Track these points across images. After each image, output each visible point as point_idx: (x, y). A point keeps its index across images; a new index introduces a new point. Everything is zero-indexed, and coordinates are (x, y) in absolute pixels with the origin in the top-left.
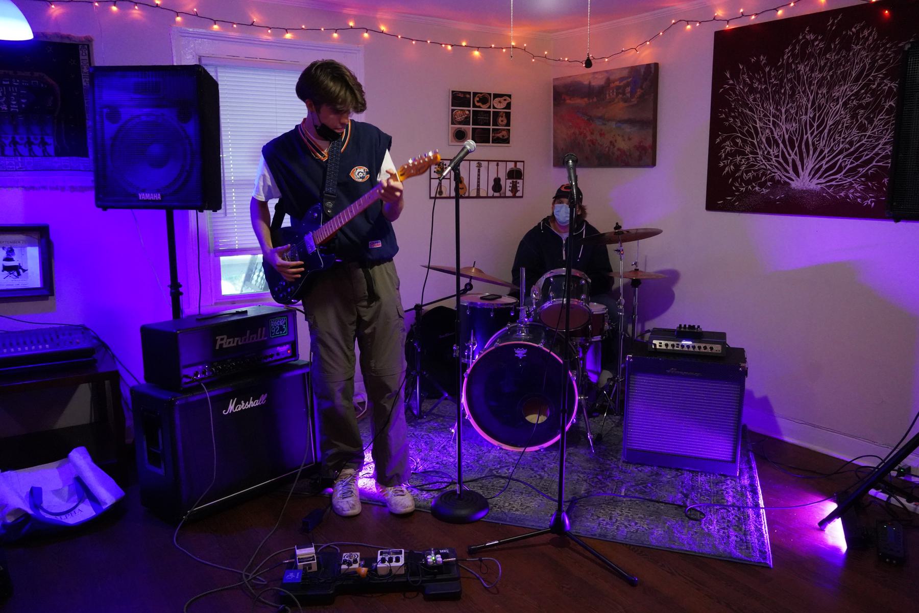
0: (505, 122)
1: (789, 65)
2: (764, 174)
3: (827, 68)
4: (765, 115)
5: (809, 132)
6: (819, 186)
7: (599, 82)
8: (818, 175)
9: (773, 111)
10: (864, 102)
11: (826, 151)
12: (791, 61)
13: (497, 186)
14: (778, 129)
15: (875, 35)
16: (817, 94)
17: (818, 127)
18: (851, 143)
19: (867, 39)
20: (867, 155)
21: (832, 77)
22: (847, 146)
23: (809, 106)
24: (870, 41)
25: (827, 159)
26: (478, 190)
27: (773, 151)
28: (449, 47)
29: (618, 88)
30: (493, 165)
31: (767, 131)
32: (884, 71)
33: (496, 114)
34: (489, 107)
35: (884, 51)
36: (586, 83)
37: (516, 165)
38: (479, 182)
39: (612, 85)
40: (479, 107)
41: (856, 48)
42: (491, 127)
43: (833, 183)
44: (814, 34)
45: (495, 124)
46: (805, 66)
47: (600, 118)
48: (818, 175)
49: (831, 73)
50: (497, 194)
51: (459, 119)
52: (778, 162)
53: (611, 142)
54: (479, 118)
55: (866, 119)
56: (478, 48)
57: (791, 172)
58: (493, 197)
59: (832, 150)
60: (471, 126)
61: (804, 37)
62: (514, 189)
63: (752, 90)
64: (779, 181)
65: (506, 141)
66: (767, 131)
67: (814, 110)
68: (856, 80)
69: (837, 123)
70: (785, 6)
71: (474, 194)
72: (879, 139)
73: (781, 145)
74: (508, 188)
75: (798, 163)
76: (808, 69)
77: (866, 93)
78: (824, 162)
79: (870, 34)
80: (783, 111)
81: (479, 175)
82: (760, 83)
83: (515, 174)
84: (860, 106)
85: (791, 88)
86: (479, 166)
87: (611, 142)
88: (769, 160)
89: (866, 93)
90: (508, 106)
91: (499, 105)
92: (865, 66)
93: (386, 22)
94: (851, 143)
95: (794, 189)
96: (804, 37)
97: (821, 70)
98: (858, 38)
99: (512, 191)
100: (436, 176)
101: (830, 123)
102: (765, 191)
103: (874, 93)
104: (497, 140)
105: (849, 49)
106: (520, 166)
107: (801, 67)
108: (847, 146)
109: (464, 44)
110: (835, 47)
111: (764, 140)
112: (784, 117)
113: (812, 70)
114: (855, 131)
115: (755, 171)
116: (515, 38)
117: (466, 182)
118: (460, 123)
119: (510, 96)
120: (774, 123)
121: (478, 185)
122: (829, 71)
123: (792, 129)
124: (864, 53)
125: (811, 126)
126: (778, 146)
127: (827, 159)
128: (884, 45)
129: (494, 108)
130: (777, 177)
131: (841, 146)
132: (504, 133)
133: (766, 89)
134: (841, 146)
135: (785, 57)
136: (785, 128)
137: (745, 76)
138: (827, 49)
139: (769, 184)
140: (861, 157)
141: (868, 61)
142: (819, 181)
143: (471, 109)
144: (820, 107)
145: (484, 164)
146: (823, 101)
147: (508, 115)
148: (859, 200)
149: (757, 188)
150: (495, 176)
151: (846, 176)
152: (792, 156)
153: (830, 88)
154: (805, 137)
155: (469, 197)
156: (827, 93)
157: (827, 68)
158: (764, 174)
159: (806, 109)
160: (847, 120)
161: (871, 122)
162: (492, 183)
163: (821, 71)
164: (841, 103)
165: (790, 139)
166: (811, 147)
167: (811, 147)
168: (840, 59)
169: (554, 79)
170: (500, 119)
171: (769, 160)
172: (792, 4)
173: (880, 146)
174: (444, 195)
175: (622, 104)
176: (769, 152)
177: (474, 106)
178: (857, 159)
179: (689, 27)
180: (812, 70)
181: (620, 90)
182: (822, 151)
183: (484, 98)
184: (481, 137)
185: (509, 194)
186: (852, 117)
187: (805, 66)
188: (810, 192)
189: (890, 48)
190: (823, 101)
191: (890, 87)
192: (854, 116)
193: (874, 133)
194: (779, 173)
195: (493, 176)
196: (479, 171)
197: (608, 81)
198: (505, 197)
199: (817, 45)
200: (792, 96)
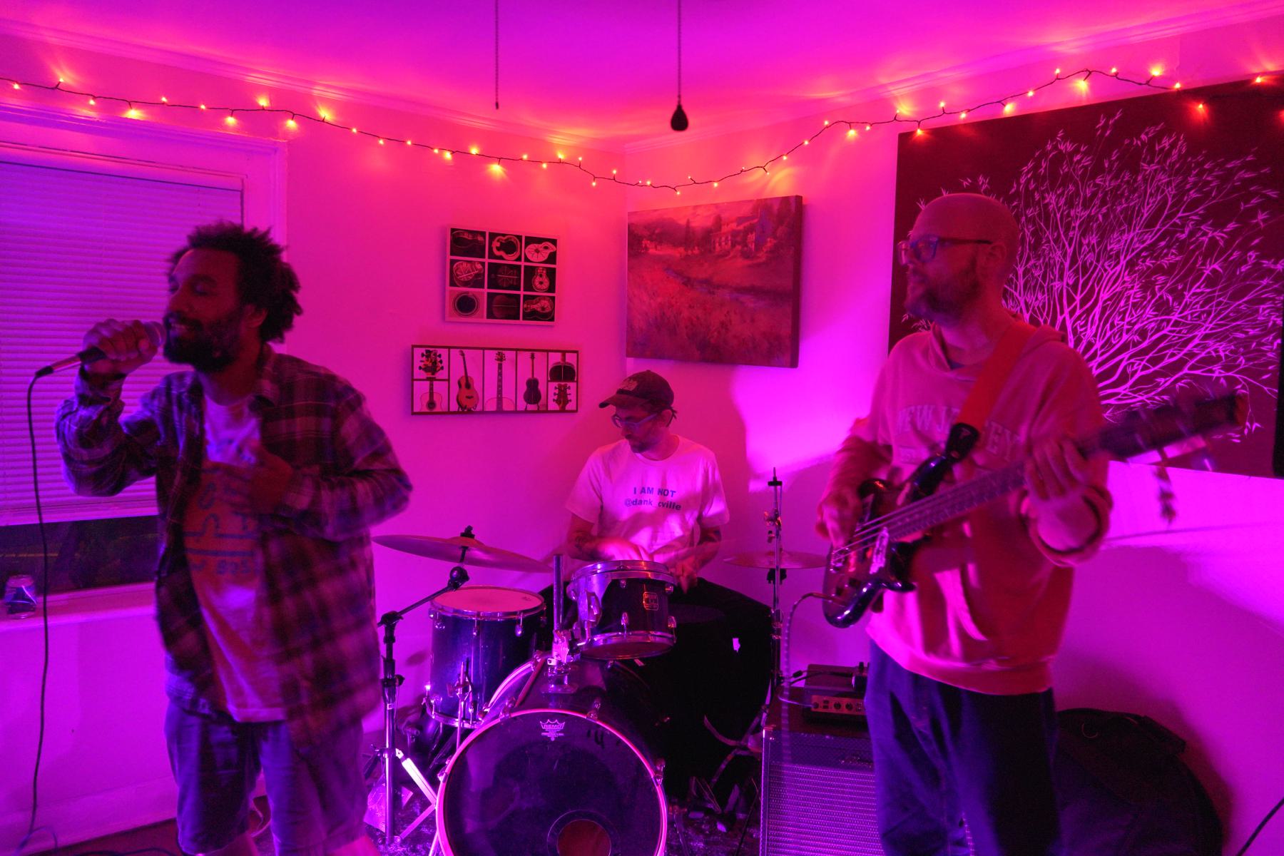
0: (546, 284)
1: (1029, 194)
3: (1097, 202)
5: (1067, 310)
7: (701, 221)
10: (1165, 262)
11: (1098, 345)
12: (1032, 186)
13: (533, 393)
14: (1010, 301)
15: (1182, 147)
16: (1081, 245)
18: (1143, 334)
19: (1168, 154)
20: (1173, 355)
21: (1106, 216)
22: (1136, 338)
23: (1067, 265)
24: (1174, 158)
26: (500, 399)
28: (448, 156)
29: (735, 234)
32: (1200, 210)
33: (531, 271)
34: (519, 259)
35: (1200, 175)
36: (683, 222)
37: (564, 359)
38: (500, 386)
39: (725, 229)
40: (501, 258)
41: (1148, 169)
42: (522, 293)
43: (1112, 401)
44: (1073, 142)
45: (529, 287)
46: (1059, 196)
47: (707, 282)
49: (1104, 210)
50: (532, 407)
51: (464, 277)
53: (722, 323)
55: (1171, 291)
56: (499, 160)
61: (1055, 148)
62: (562, 398)
65: (548, 316)
67: (1076, 272)
68: (1150, 224)
69: (1116, 298)
70: (1017, 95)
71: (491, 407)
74: (552, 397)
76: (1063, 201)
77: (1168, 246)
79: (1173, 146)
80: (1020, 272)
81: (500, 374)
83: (564, 373)
84: (1159, 270)
85: (1034, 233)
86: (501, 358)
87: (722, 323)
89: (1168, 246)
90: (552, 258)
91: (536, 257)
93: (329, 103)
94: (1143, 334)
97: (1086, 205)
98: (1152, 152)
99: (558, 401)
100: (424, 375)
101: (1105, 295)
103: (1182, 246)
104: (532, 315)
105: (1135, 171)
106: (571, 359)
107: (1051, 198)
108: (1136, 338)
109: (474, 151)
110: (1111, 165)
112: (1022, 282)
113: (1070, 204)
114: (1150, 312)
116: (564, 147)
117: (477, 385)
118: (466, 284)
119: (554, 242)
121: (500, 392)
124: (1164, 178)
125: (1071, 300)
127: (1099, 359)
128: (1200, 165)
129: (527, 260)
131: (1125, 337)
132: (545, 303)
134: (1125, 337)
135: (1023, 180)
138: (1098, 169)
140: (1162, 358)
141: (1171, 192)
143: (487, 260)
144: (1085, 270)
145: (509, 355)
146: (1091, 258)
147: (551, 274)
151: (1136, 387)
153: (1104, 235)
154: (1060, 318)
155: (483, 412)
156: (1099, 243)
157: (1097, 202)
159: (1062, 270)
160: (1135, 293)
161: (1179, 297)
162: (523, 388)
163: (1085, 207)
164: (1123, 262)
168: (1120, 186)
169: (630, 214)
170: (537, 280)
172: (1031, 94)
173: (1196, 341)
174: (437, 409)
175: (740, 262)
177: (492, 256)
178: (1154, 361)
179: (852, 133)
180: (1070, 204)
181: (738, 239)
182: (1090, 345)
183: (509, 245)
184: (505, 309)
185: (553, 406)
186: (1145, 288)
187: (1059, 196)
189: (1211, 171)
190: (1091, 258)
191: (1212, 239)
192: (1147, 286)
193: (1185, 317)
195: (525, 375)
196: (500, 367)
197: (719, 221)
198: (547, 411)
199: (1079, 162)
200: (1036, 247)
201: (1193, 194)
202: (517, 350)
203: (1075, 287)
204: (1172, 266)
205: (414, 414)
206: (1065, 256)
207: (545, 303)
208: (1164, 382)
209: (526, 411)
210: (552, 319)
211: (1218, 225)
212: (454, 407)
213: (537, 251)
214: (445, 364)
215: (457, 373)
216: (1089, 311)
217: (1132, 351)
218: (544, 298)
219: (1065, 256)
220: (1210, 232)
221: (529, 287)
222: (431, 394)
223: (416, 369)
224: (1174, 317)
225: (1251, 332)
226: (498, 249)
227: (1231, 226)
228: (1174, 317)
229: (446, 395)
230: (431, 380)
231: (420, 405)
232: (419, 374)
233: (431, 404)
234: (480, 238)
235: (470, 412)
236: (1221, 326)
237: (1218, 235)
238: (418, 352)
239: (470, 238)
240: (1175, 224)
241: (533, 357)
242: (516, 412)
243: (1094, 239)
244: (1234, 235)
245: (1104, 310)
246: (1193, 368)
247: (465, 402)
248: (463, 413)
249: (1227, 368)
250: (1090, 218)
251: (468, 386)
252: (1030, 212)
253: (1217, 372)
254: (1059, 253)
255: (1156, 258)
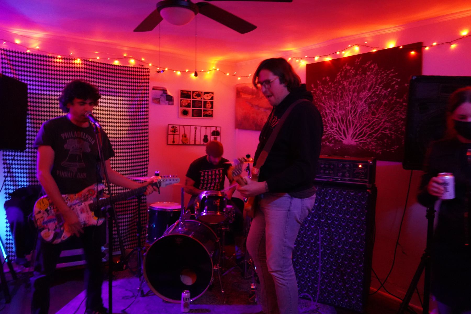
0: (210, 106)
2: (331, 136)
4: (330, 107)
6: (356, 143)
8: (355, 137)
9: (334, 104)
11: (358, 125)
12: (340, 79)
16: (353, 96)
17: (354, 112)
19: (373, 69)
21: (359, 87)
22: (368, 123)
23: (349, 102)
24: (375, 70)
25: (358, 129)
26: (195, 141)
27: (334, 125)
30: (203, 129)
31: (331, 114)
32: (382, 85)
33: (205, 102)
34: (202, 99)
35: (381, 75)
40: (196, 98)
42: (203, 109)
45: (205, 107)
47: (257, 106)
48: (355, 137)
49: (358, 86)
50: (205, 143)
51: (184, 104)
52: (337, 130)
54: (195, 104)
57: (343, 135)
58: (203, 145)
59: (361, 125)
60: (191, 108)
61: (345, 68)
63: (324, 94)
64: (337, 140)
65: (211, 116)
66: (331, 114)
67: (352, 104)
68: (370, 89)
69: (362, 111)
72: (382, 119)
73: (338, 122)
75: (346, 131)
76: (348, 83)
78: (357, 131)
79: (374, 67)
80: (338, 104)
81: (195, 133)
82: (327, 90)
86: (196, 129)
88: (333, 129)
89: (374, 96)
90: (212, 98)
92: (373, 82)
94: (369, 121)
95: (345, 145)
96: (345, 68)
97: (354, 84)
100: (172, 133)
101: (359, 111)
102: (331, 145)
104: (206, 116)
105: (365, 74)
106: (218, 129)
107: (345, 83)
111: (330, 119)
112: (338, 107)
113: (350, 84)
114: (371, 115)
115: (327, 135)
117: (188, 136)
118: (185, 107)
119: (213, 93)
120: (334, 111)
122: (358, 84)
123: (343, 114)
124: (372, 76)
125: (351, 112)
126: (336, 122)
127: (358, 129)
130: (337, 138)
131: (365, 122)
133: (330, 93)
134: (365, 122)
135: (338, 77)
136: (339, 113)
137: (320, 87)
138: (356, 74)
139: (333, 141)
141: (374, 80)
142: (356, 140)
143: (192, 99)
145: (199, 128)
147: (212, 103)
148: (374, 150)
149: (328, 144)
150: (204, 134)
152: (343, 127)
153: (359, 93)
156: (357, 95)
158: (331, 136)
159: (348, 104)
161: (377, 111)
162: (203, 138)
164: (363, 101)
165: (342, 119)
166: (351, 123)
167: (351, 123)
168: (361, 79)
170: (207, 105)
171: (333, 129)
176: (332, 125)
177: (193, 98)
180: (350, 84)
182: (356, 125)
183: (199, 94)
184: (197, 114)
188: (351, 146)
189: (384, 74)
191: (385, 93)
192: (370, 108)
194: (337, 136)
195: (203, 134)
196: (196, 131)
200: (342, 97)
201: (380, 81)
202: (201, 126)
203: (352, 108)
204: (376, 101)
205: (168, 144)
206: (349, 99)
207: (210, 112)
208: (375, 135)
209: (203, 145)
210: (212, 117)
211: (386, 90)
212: (181, 143)
213: (207, 96)
214: (178, 130)
215: (182, 133)
216: (355, 115)
217: (367, 126)
218: (210, 110)
219: (349, 99)
220: (384, 92)
221: (205, 107)
222: (174, 139)
223: (169, 132)
224: (377, 116)
225: (396, 120)
226: (195, 96)
227: (389, 89)
228: (377, 116)
229: (178, 139)
230: (174, 135)
231: (170, 142)
232: (170, 133)
233: (174, 142)
234: (189, 93)
235: (186, 145)
236: (387, 118)
237: (386, 92)
238: (170, 126)
239: (186, 93)
240: (376, 90)
241: (206, 128)
242: (200, 145)
243: (356, 94)
244: (390, 92)
245: (359, 114)
246: (382, 131)
247: (184, 141)
248: (183, 145)
249: (390, 130)
250: (355, 88)
251: (185, 136)
252: (340, 87)
253: (388, 132)
254: (347, 98)
255: (371, 99)
